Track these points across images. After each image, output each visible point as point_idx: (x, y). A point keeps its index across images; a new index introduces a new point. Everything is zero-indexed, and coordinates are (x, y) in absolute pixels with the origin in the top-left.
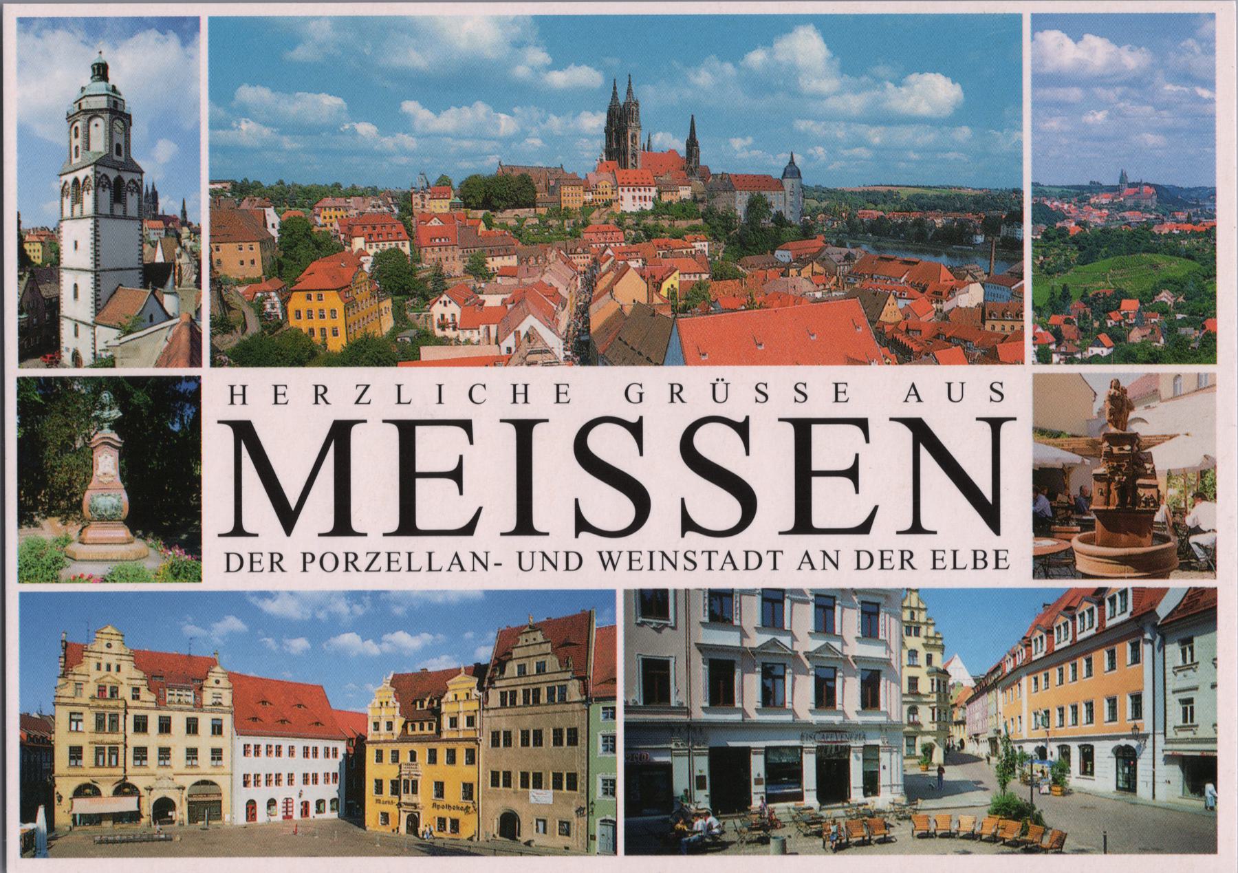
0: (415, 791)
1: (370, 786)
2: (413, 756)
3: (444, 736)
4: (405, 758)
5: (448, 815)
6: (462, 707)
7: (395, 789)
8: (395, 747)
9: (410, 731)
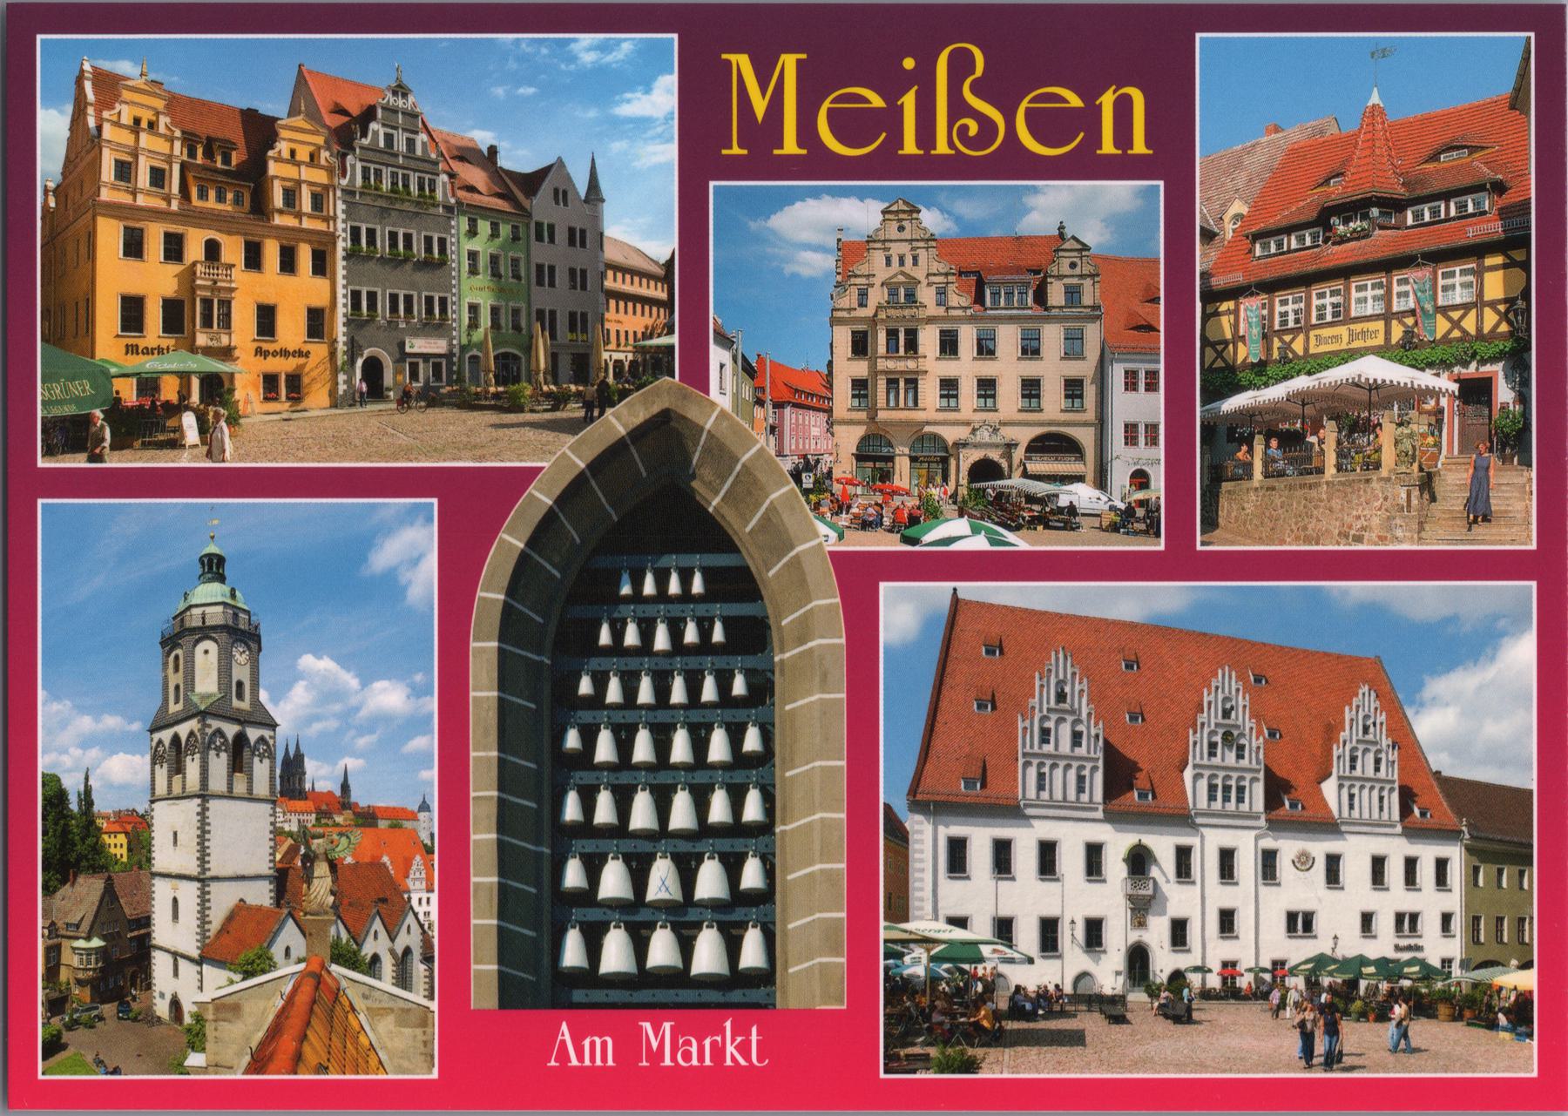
0: (226, 322)
1: (108, 316)
2: (212, 250)
3: (278, 220)
4: (194, 250)
5: (283, 366)
7: (174, 316)
9: (196, 202)
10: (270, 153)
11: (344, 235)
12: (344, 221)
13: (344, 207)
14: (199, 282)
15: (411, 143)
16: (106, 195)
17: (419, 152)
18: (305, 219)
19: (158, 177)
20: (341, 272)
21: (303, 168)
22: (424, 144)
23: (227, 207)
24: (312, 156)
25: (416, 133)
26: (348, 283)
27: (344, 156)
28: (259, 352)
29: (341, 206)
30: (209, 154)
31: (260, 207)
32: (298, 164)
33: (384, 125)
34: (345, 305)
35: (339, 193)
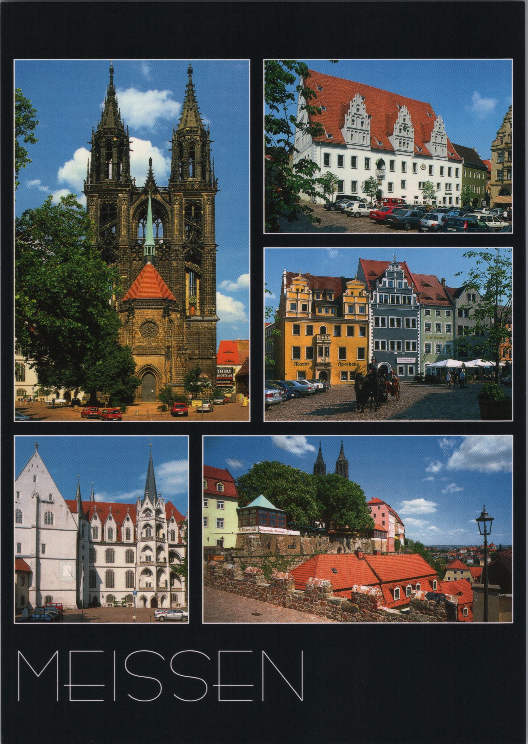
0: (327, 354)
1: (289, 353)
2: (323, 330)
3: (346, 318)
4: (317, 331)
6: (357, 300)
7: (310, 352)
8: (311, 324)
9: (318, 314)
10: (344, 294)
11: (372, 321)
12: (372, 316)
14: (318, 341)
15: (400, 284)
16: (287, 315)
17: (403, 287)
18: (356, 316)
19: (304, 307)
20: (371, 335)
22: (405, 283)
23: (330, 314)
25: (402, 280)
26: (374, 339)
27: (372, 292)
28: (339, 364)
29: (371, 310)
30: (324, 296)
31: (340, 313)
32: (354, 297)
35: (370, 306)
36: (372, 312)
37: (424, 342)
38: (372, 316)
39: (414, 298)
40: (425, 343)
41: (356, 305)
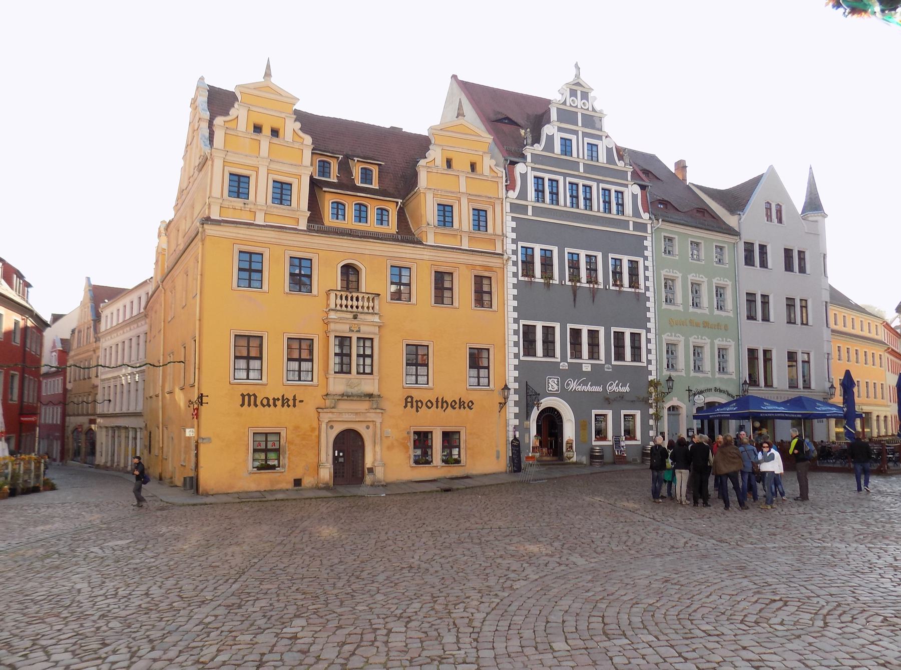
11: (514, 258)
12: (514, 241)
13: (514, 224)
19: (282, 192)
21: (463, 180)
24: (473, 166)
27: (513, 163)
28: (409, 401)
33: (560, 129)
34: (516, 344)
36: (513, 230)
37: (664, 337)
38: (514, 241)
39: (635, 197)
40: (666, 337)
41: (464, 201)
